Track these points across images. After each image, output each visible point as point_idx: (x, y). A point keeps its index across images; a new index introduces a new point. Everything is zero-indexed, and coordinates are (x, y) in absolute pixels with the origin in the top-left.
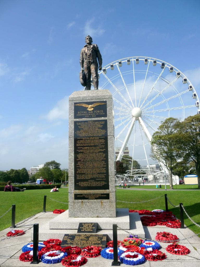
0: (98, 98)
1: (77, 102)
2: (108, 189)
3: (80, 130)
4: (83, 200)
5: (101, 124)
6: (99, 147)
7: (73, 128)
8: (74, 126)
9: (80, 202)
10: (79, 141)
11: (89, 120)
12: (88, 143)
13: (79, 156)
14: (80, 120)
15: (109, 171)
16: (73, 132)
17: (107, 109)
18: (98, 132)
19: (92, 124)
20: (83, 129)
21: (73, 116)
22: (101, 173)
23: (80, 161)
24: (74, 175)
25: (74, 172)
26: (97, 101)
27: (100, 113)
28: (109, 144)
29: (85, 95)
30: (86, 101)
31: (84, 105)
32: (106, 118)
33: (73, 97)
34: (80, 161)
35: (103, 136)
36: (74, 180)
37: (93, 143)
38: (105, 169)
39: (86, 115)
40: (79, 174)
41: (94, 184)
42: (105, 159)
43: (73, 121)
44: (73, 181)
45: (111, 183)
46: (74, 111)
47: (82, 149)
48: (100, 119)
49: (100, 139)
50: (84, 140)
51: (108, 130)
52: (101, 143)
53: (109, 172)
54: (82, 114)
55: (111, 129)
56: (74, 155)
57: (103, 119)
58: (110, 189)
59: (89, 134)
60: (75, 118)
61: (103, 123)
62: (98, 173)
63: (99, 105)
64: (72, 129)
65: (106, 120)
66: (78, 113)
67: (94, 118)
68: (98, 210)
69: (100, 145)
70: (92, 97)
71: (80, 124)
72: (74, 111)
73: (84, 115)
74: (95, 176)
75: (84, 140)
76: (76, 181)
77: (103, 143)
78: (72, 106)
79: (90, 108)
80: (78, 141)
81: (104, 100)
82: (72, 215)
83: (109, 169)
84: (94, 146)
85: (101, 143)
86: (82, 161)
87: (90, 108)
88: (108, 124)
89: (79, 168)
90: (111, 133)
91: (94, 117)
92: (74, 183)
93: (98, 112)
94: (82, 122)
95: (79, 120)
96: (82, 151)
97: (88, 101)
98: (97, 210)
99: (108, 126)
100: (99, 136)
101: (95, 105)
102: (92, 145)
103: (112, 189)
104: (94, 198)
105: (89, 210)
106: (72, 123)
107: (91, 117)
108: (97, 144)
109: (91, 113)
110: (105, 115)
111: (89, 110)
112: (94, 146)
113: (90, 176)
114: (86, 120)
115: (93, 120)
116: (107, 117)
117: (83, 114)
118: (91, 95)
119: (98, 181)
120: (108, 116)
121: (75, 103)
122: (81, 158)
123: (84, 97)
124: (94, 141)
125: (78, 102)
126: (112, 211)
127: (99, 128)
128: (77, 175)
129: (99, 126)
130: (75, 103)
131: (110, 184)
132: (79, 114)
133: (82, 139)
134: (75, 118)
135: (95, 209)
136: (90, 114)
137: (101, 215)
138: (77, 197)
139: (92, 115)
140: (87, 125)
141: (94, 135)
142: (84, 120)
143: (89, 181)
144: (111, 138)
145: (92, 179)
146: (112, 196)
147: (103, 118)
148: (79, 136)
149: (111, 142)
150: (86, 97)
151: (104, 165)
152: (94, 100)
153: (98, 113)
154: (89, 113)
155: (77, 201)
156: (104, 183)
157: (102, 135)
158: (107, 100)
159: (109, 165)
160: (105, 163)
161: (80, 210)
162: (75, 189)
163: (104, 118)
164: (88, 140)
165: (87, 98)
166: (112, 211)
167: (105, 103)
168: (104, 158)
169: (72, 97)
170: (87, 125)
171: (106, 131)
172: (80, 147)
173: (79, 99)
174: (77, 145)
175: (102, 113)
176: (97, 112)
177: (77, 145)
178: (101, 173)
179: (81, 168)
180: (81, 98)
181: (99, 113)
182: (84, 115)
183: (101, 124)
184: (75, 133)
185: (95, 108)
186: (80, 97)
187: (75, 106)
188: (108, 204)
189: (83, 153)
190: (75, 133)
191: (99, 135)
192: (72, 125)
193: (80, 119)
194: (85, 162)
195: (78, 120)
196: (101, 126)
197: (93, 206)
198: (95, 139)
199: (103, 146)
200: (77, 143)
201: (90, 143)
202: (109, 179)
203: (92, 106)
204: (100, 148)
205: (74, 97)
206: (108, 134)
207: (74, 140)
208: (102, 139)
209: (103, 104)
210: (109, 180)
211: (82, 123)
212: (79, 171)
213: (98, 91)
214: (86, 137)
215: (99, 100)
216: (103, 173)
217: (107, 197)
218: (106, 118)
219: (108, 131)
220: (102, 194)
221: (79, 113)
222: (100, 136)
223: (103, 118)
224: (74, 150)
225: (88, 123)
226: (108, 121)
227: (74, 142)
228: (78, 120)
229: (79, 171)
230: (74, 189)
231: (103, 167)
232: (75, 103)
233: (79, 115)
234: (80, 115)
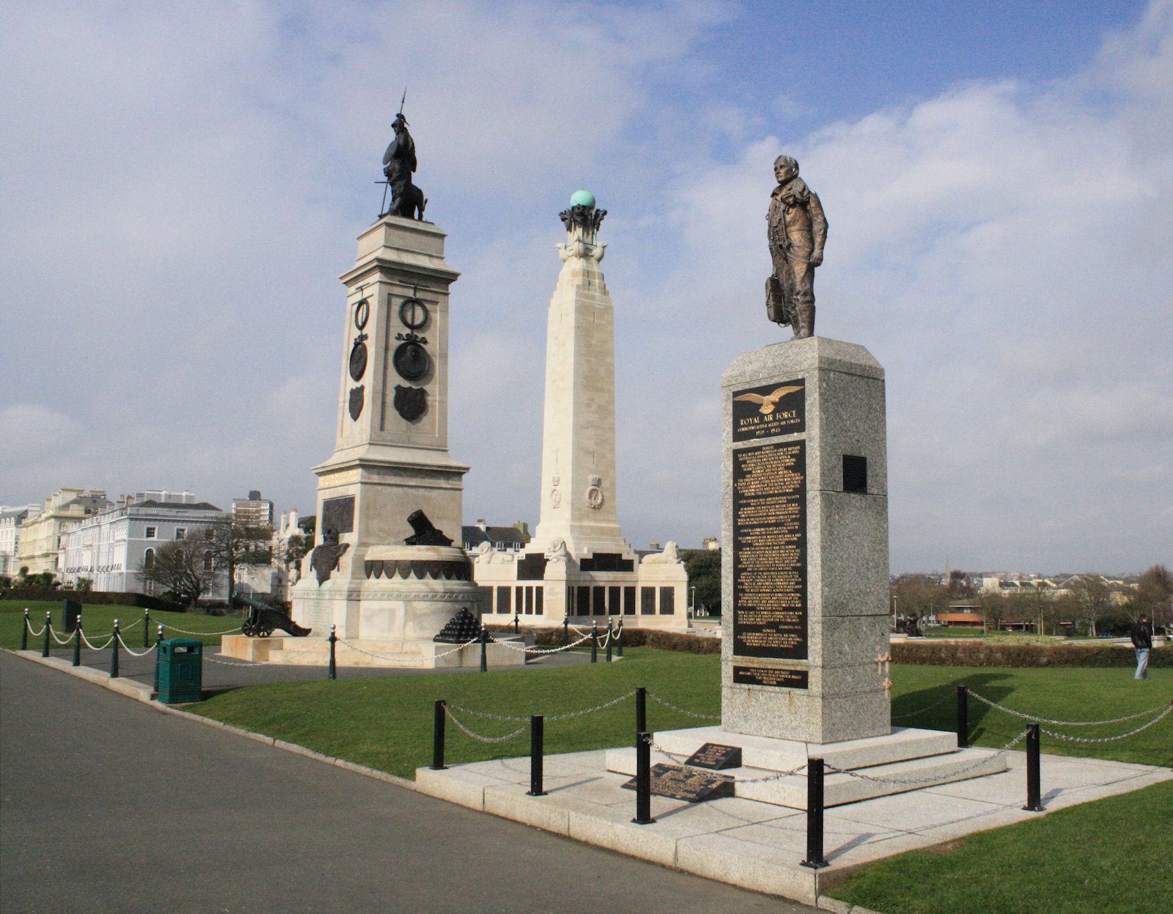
2: (806, 658)
4: (751, 686)
5: (792, 456)
6: (787, 526)
7: (731, 470)
9: (745, 690)
13: (745, 555)
14: (745, 447)
15: (809, 602)
17: (806, 404)
19: (770, 455)
20: (750, 472)
21: (731, 435)
24: (732, 611)
25: (732, 602)
26: (782, 381)
28: (808, 518)
30: (757, 385)
31: (754, 398)
35: (796, 491)
36: (732, 625)
38: (798, 595)
39: (757, 430)
40: (743, 608)
41: (775, 640)
42: (799, 565)
44: (731, 630)
45: (814, 640)
47: (748, 534)
49: (789, 501)
51: (807, 473)
52: (793, 514)
53: (809, 606)
54: (749, 425)
56: (732, 553)
58: (810, 658)
60: (734, 440)
61: (796, 450)
62: (785, 609)
63: (788, 394)
68: (781, 719)
72: (731, 419)
74: (779, 616)
77: (796, 514)
82: (728, 726)
83: (809, 596)
84: (776, 525)
86: (749, 572)
89: (743, 591)
90: (815, 483)
91: (775, 434)
92: (732, 634)
97: (764, 383)
98: (780, 717)
102: (772, 520)
103: (814, 659)
104: (775, 683)
105: (764, 716)
108: (782, 517)
112: (776, 525)
113: (767, 616)
115: (773, 443)
116: (804, 431)
120: (807, 426)
122: (747, 560)
125: (740, 388)
126: (813, 723)
128: (739, 612)
130: (736, 394)
131: (809, 644)
133: (748, 505)
135: (776, 714)
137: (788, 735)
138: (741, 676)
143: (764, 631)
144: (813, 499)
145: (771, 625)
146: (813, 680)
148: (742, 496)
151: (797, 583)
155: (738, 685)
156: (794, 639)
159: (809, 584)
160: (800, 577)
161: (745, 715)
164: (764, 505)
165: (761, 375)
166: (813, 723)
167: (803, 387)
168: (798, 561)
169: (729, 374)
171: (802, 477)
175: (794, 419)
177: (739, 524)
179: (747, 593)
180: (748, 377)
181: (786, 420)
183: (792, 456)
184: (736, 485)
185: (780, 406)
188: (804, 703)
189: (750, 545)
192: (729, 463)
194: (756, 573)
195: (740, 445)
196: (791, 462)
197: (771, 704)
199: (795, 526)
201: (767, 516)
202: (809, 627)
204: (791, 532)
206: (809, 486)
209: (794, 389)
210: (809, 632)
215: (788, 378)
216: (794, 609)
217: (800, 680)
219: (808, 478)
220: (792, 672)
221: (745, 426)
223: (796, 434)
226: (806, 444)
230: (732, 652)
231: (796, 591)
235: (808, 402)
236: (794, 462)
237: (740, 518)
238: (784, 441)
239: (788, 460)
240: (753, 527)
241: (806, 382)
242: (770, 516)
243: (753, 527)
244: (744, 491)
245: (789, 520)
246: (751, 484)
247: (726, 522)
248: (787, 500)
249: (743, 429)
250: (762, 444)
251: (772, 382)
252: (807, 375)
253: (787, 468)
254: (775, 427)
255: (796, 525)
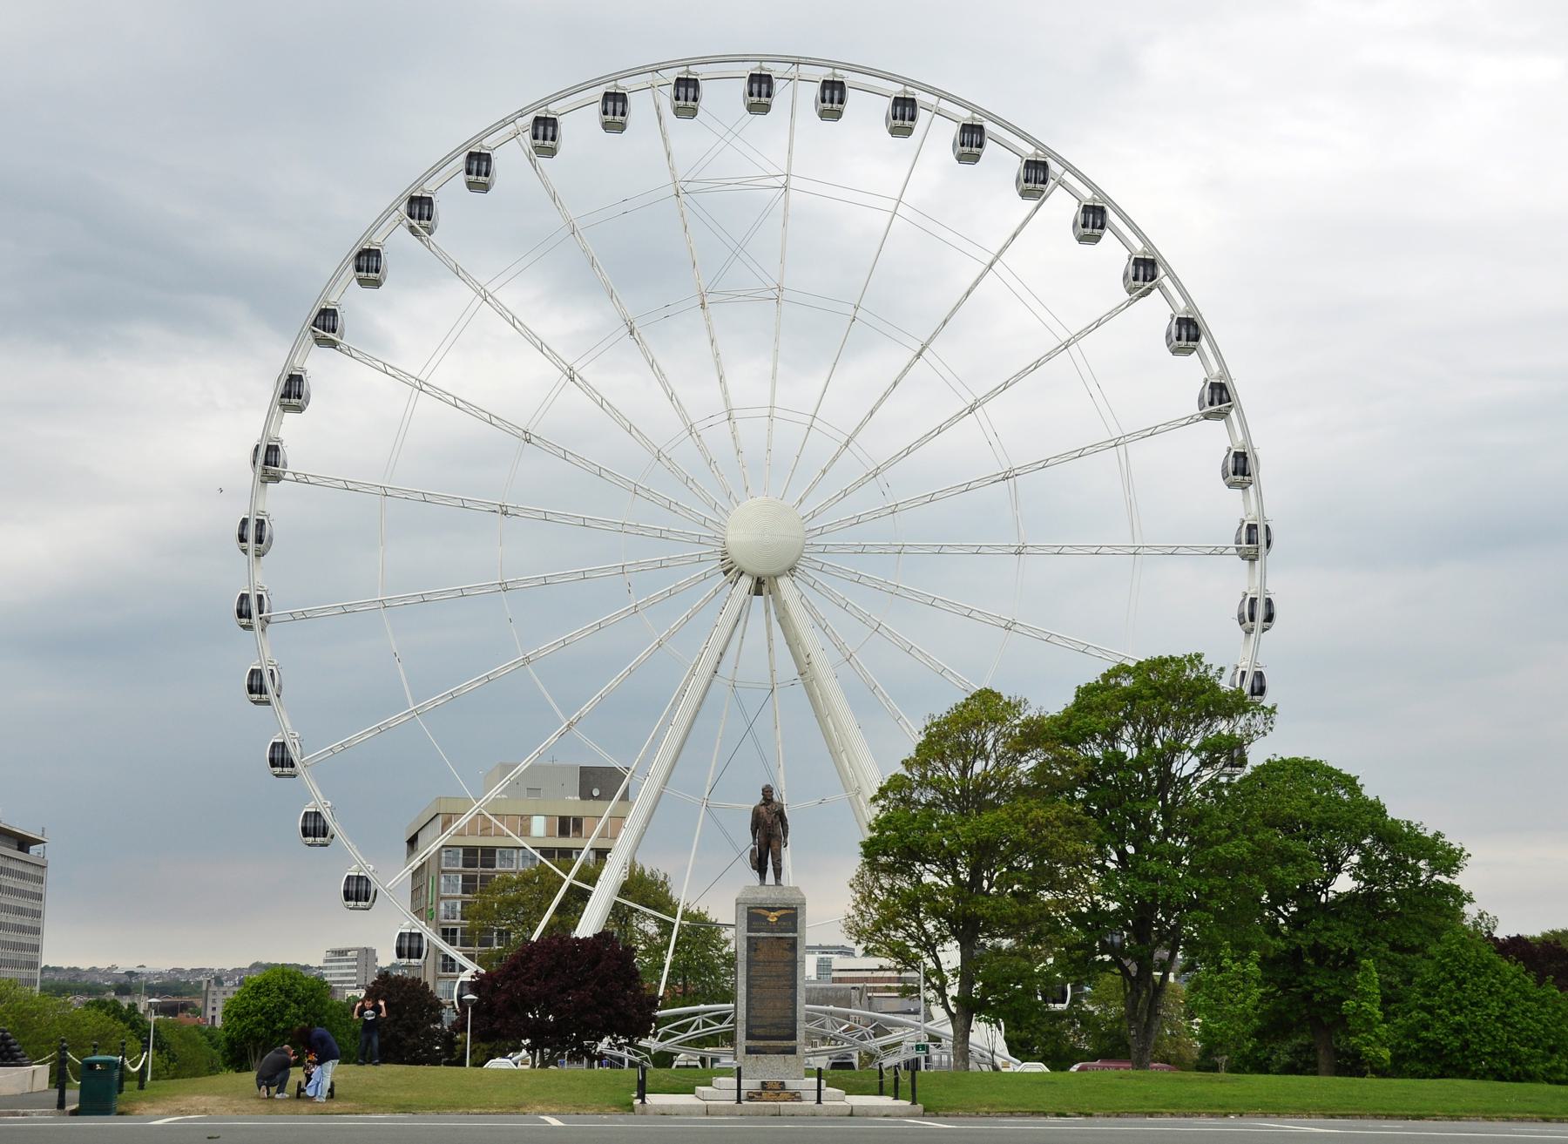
7: (746, 946)
16: (746, 953)
17: (799, 920)
22: (786, 1017)
23: (755, 998)
29: (764, 896)
30: (765, 906)
32: (795, 935)
34: (755, 998)
40: (752, 1017)
41: (775, 1032)
60: (748, 931)
61: (791, 941)
74: (777, 1021)
76: (749, 1027)
79: (772, 918)
84: (778, 976)
87: (773, 917)
89: (754, 1008)
93: (784, 923)
94: (759, 937)
96: (758, 982)
97: (770, 906)
102: (774, 974)
110: (795, 931)
118: (773, 896)
119: (780, 1028)
134: (748, 931)
145: (772, 1025)
147: (791, 935)
150: (766, 899)
155: (749, 1055)
156: (787, 1031)
162: (747, 1038)
178: (786, 1017)
186: (756, 898)
195: (753, 934)
197: (772, 1063)
203: (776, 914)
206: (798, 959)
209: (792, 912)
212: (753, 1013)
216: (789, 1017)
218: (795, 935)
221: (755, 925)
228: (753, 934)
229: (753, 1013)
230: (744, 1039)
251: (776, 906)
255: (791, 977)
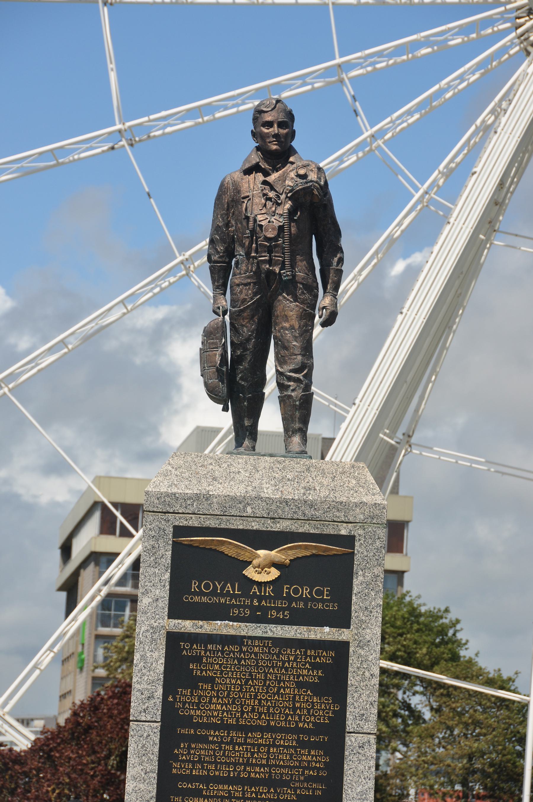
0: (310, 512)
1: (191, 523)
3: (197, 688)
7: (162, 668)
8: (162, 661)
10: (189, 748)
11: (250, 634)
12: (235, 764)
14: (199, 631)
16: (160, 691)
17: (356, 582)
18: (294, 709)
20: (211, 680)
21: (164, 603)
26: (301, 530)
27: (313, 599)
28: (348, 778)
30: (239, 525)
32: (344, 635)
33: (167, 495)
35: (319, 729)
37: (261, 766)
39: (234, 606)
43: (163, 632)
46: (171, 573)
48: (312, 636)
49: (302, 744)
50: (213, 742)
51: (349, 700)
52: (309, 768)
54: (214, 593)
55: (364, 697)
57: (329, 638)
59: (242, 713)
60: (171, 616)
63: (313, 555)
64: (153, 676)
65: (346, 645)
66: (194, 586)
67: (279, 627)
69: (299, 781)
70: (274, 507)
71: (197, 649)
72: (167, 575)
73: (223, 600)
75: (213, 742)
77: (319, 769)
78: (161, 543)
79: (261, 568)
80: (179, 747)
81: (343, 532)
85: (304, 768)
88: (350, 669)
93: (305, 592)
94: (210, 638)
95: (193, 631)
97: (255, 526)
99: (351, 680)
100: (297, 731)
101: (290, 552)
102: (258, 773)
106: (153, 640)
107: (263, 619)
109: (265, 598)
111: (257, 578)
114: (232, 632)
115: (270, 634)
116: (349, 627)
117: (222, 595)
118: (268, 491)
120: (354, 620)
121: (176, 528)
123: (233, 499)
124: (268, 752)
125: (194, 522)
127: (300, 685)
129: (305, 672)
130: (179, 531)
132: (195, 593)
133: (204, 740)
134: (171, 616)
136: (260, 598)
139: (272, 608)
140: (239, 660)
141: (272, 723)
142: (224, 632)
148: (188, 722)
149: (361, 767)
150: (244, 501)
152: (288, 523)
153: (301, 598)
154: (255, 595)
157: (314, 724)
158: (358, 532)
163: (334, 630)
164: (240, 744)
165: (249, 510)
170: (239, 660)
172: (190, 778)
173: (204, 508)
174: (174, 771)
176: (296, 591)
177: (174, 771)
181: (306, 601)
182: (223, 600)
183: (315, 666)
184: (170, 699)
186: (208, 497)
187: (176, 546)
190: (170, 699)
191: (301, 725)
192: (156, 655)
193: (201, 623)
198: (274, 745)
199: (314, 790)
200: (176, 758)
201: (247, 764)
203: (274, 554)
205: (175, 490)
206: (351, 724)
207: (157, 742)
208: (316, 746)
209: (336, 549)
211: (209, 647)
213: (308, 470)
214: (228, 727)
218: (344, 635)
219: (350, 709)
222: (303, 731)
223: (327, 629)
224: (154, 793)
225: (241, 651)
226: (351, 649)
227: (156, 749)
232: (176, 528)
233: (197, 599)
234: (204, 599)
235: (361, 578)
236: (319, 678)
237: (176, 760)
238: (299, 636)
239: (305, 672)
240: (207, 780)
241: (357, 544)
242: (256, 765)
243: (207, 780)
244: (192, 712)
245: (302, 778)
246: (210, 702)
247: (141, 764)
248: (298, 741)
249: (197, 599)
250: (243, 633)
252: (361, 532)
253: (300, 685)
254: (278, 610)
